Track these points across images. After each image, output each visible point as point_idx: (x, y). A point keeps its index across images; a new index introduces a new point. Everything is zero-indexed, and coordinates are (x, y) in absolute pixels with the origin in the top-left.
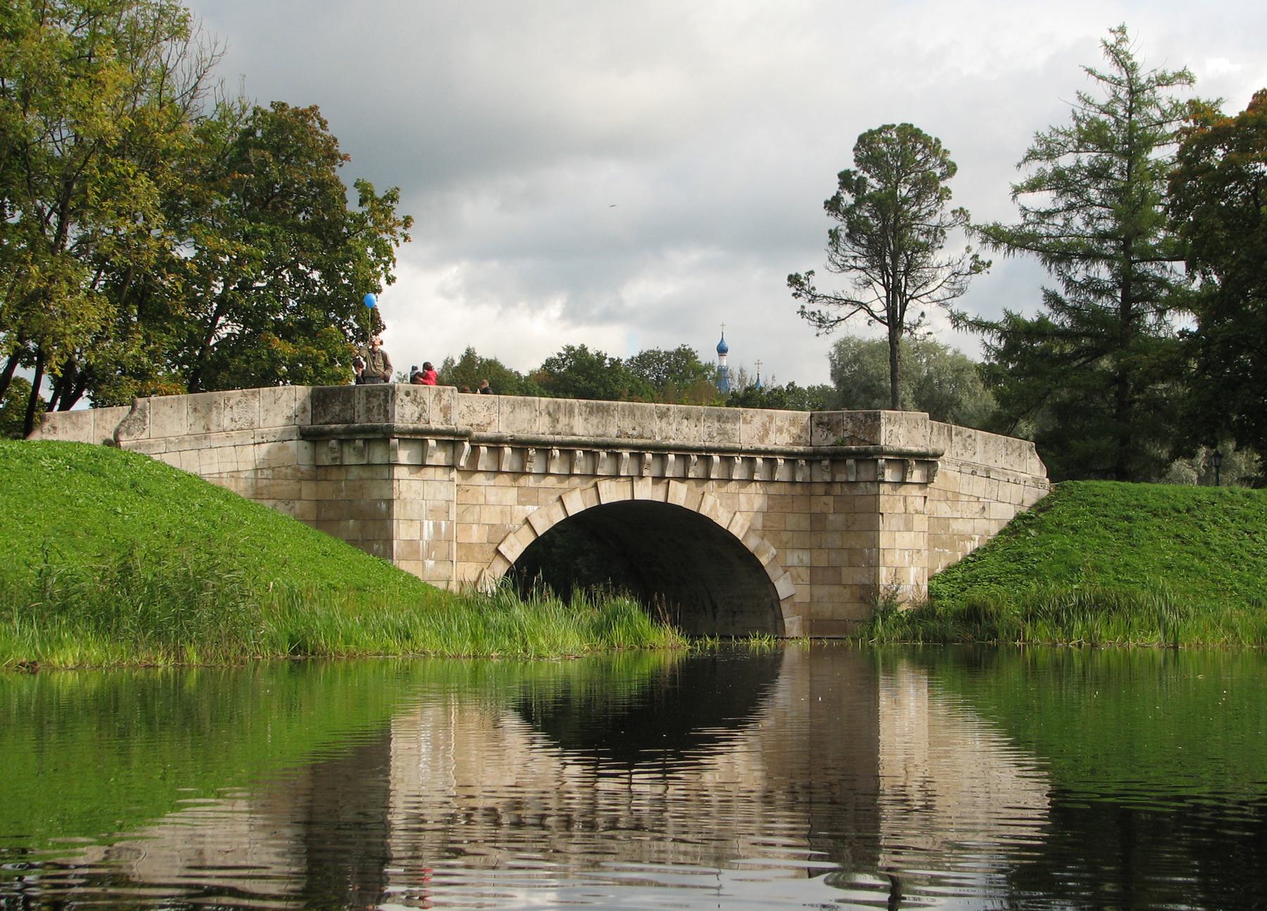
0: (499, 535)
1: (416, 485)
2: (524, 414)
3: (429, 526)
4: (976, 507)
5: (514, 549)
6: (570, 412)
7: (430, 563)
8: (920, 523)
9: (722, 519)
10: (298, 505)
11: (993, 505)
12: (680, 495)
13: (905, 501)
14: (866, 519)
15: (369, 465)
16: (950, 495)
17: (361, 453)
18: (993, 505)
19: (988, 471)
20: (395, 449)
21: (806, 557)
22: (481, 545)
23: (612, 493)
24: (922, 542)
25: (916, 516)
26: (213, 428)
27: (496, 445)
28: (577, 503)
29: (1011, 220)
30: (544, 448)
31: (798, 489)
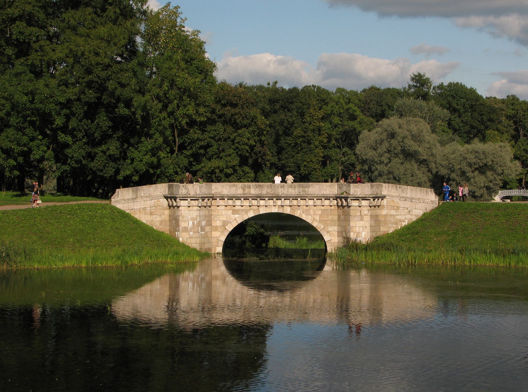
0: (225, 224)
1: (186, 212)
2: (234, 189)
3: (191, 223)
4: (406, 211)
5: (230, 228)
6: (249, 187)
7: (191, 233)
8: (367, 218)
9: (304, 217)
10: (163, 216)
12: (287, 211)
13: (360, 211)
16: (395, 208)
22: (220, 226)
23: (263, 211)
24: (368, 225)
25: (365, 216)
26: (139, 196)
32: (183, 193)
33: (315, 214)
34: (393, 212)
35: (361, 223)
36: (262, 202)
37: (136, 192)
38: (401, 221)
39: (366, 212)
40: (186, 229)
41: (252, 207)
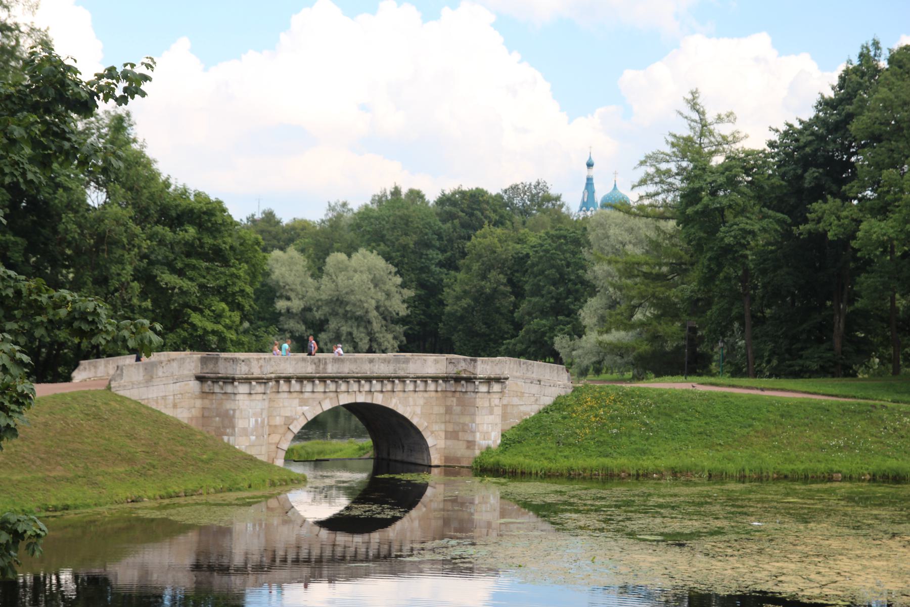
0: (289, 421)
1: (247, 403)
3: (253, 421)
4: (533, 399)
7: (253, 438)
8: (498, 411)
9: (400, 410)
10: (193, 410)
11: (542, 398)
12: (378, 399)
14: (468, 408)
15: (226, 393)
17: (222, 389)
18: (542, 398)
19: (539, 381)
20: (236, 387)
21: (443, 427)
22: (281, 426)
23: (345, 399)
24: (498, 420)
27: (288, 379)
30: (311, 379)
31: (439, 394)
32: (243, 372)
33: (415, 405)
34: (515, 401)
35: (490, 419)
36: (343, 387)
37: (150, 371)
38: (525, 414)
39: (497, 401)
40: (245, 432)
41: (328, 394)
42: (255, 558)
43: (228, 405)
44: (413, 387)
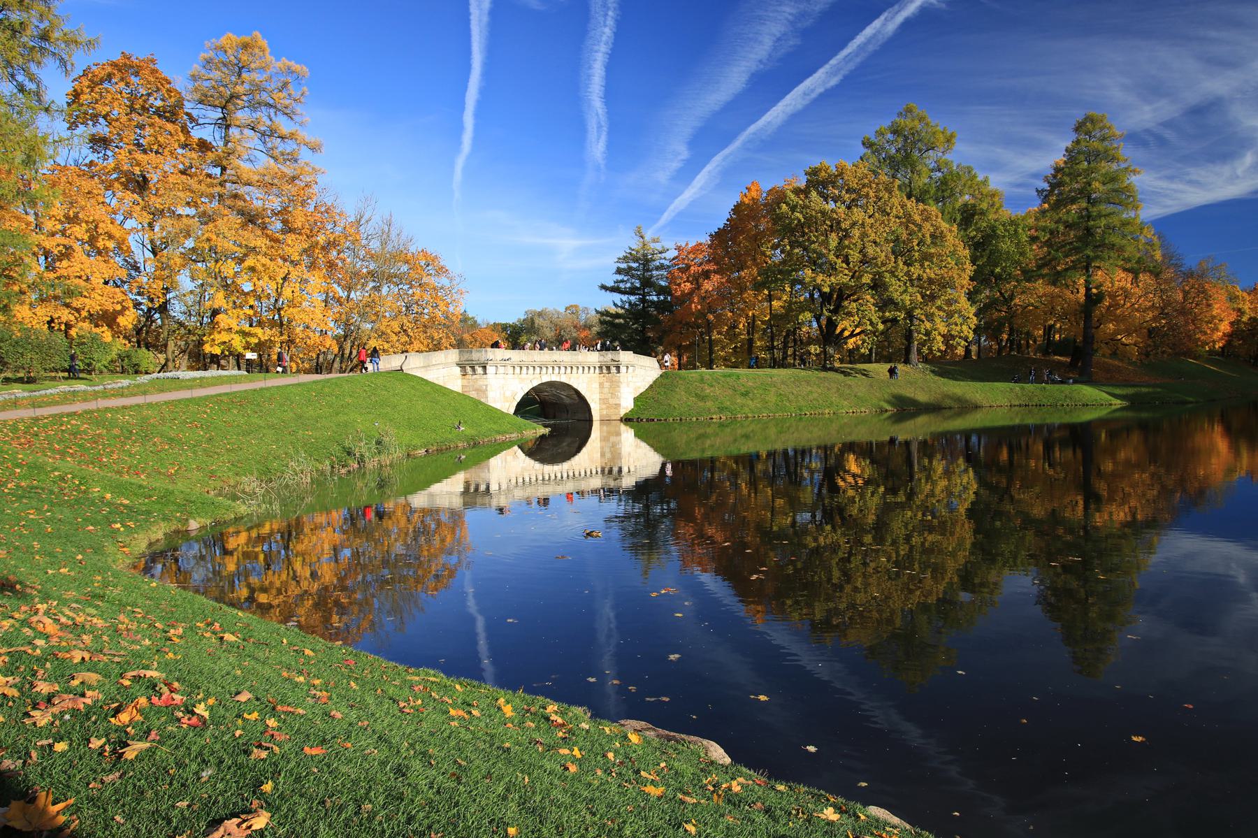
12: (564, 379)
14: (615, 385)
28: (535, 384)
29: (610, 284)
42: (504, 487)
43: (480, 383)
44: (581, 371)
